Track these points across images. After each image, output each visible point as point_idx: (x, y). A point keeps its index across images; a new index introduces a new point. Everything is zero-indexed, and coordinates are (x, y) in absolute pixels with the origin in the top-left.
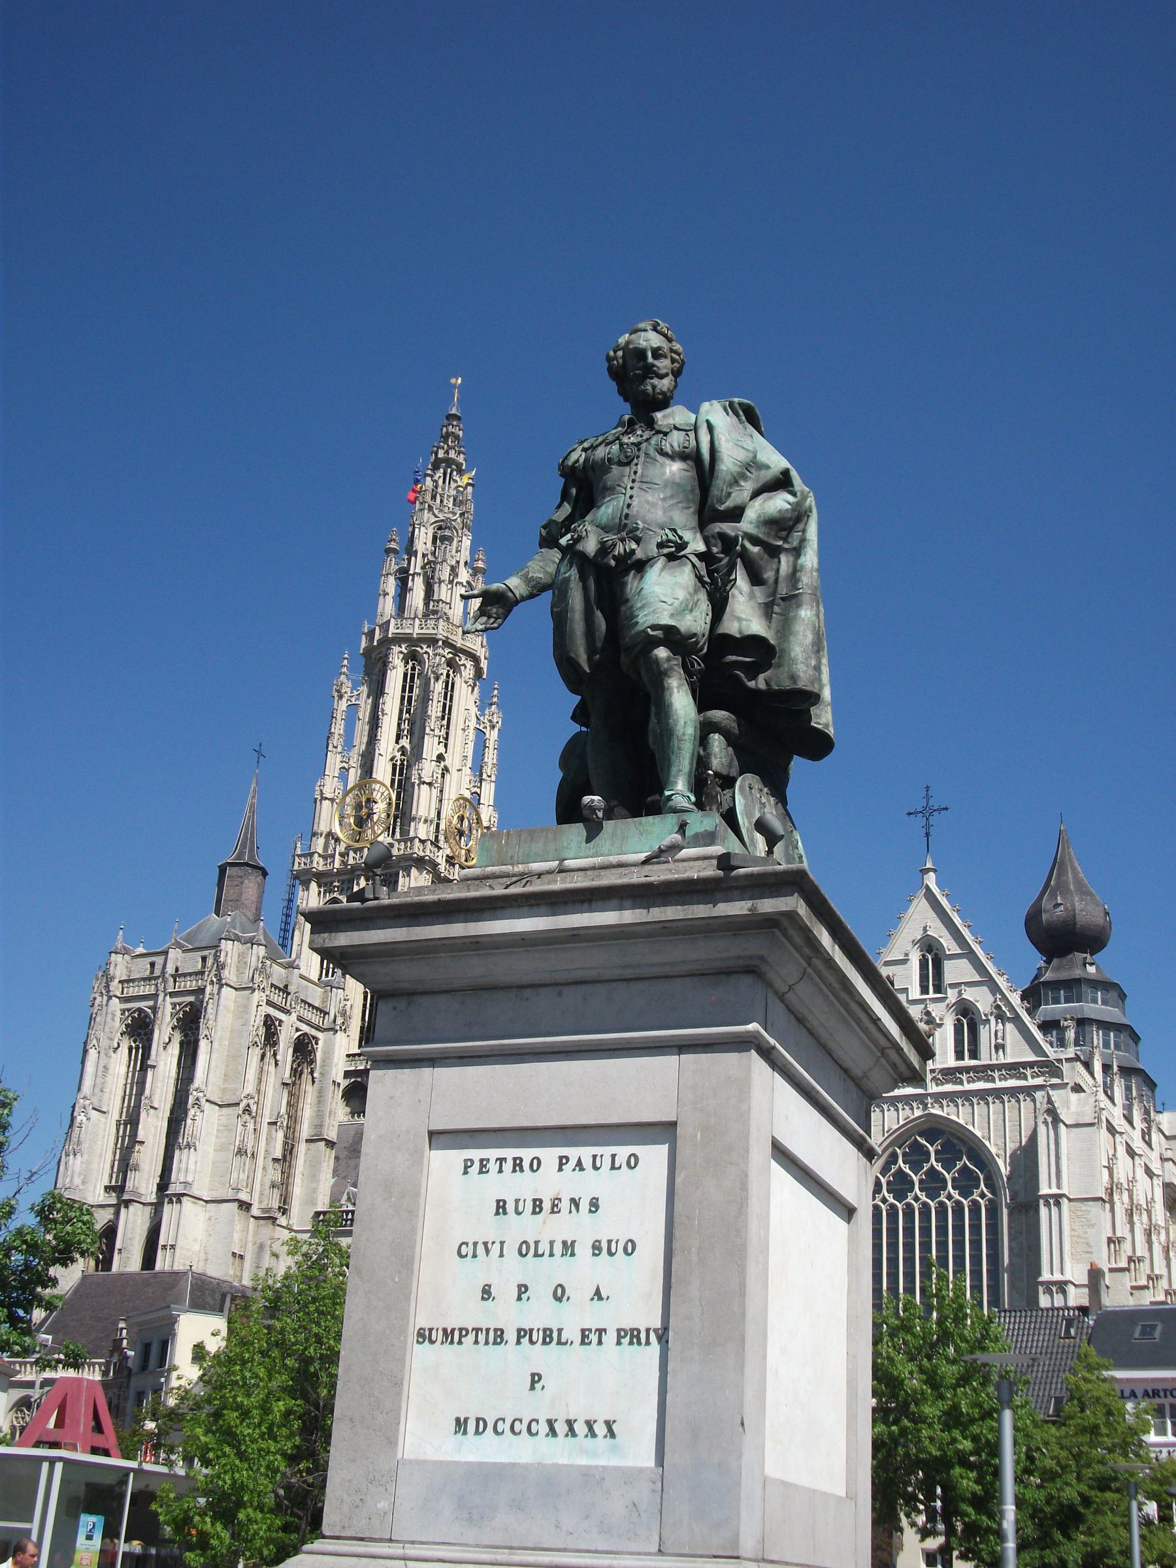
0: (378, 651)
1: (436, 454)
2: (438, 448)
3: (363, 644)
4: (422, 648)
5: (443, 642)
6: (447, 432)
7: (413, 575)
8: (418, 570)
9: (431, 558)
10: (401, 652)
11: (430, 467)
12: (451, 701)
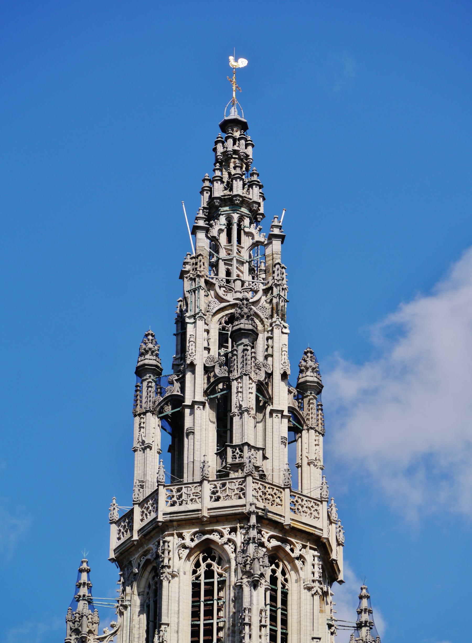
0: (141, 551)
1: (210, 190)
2: (212, 182)
3: (114, 543)
4: (222, 536)
5: (260, 519)
6: (224, 153)
7: (191, 407)
8: (200, 397)
9: (219, 372)
10: (184, 547)
11: (201, 215)
12: (284, 622)
